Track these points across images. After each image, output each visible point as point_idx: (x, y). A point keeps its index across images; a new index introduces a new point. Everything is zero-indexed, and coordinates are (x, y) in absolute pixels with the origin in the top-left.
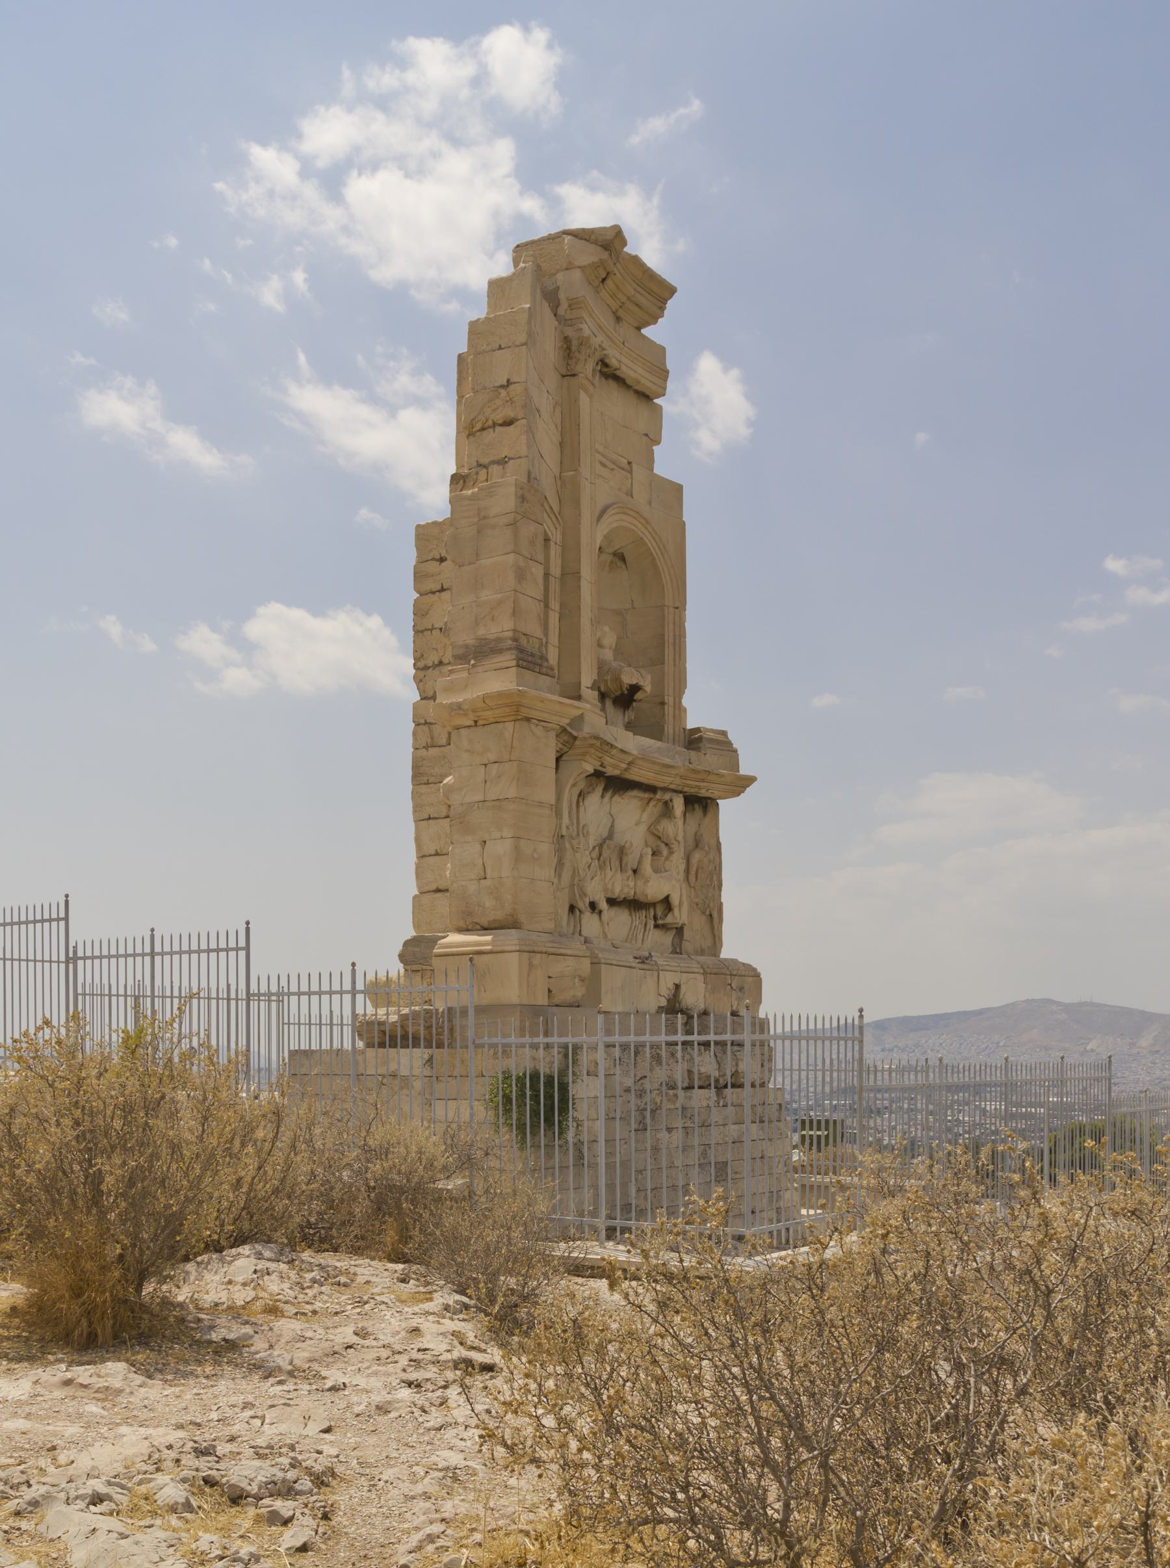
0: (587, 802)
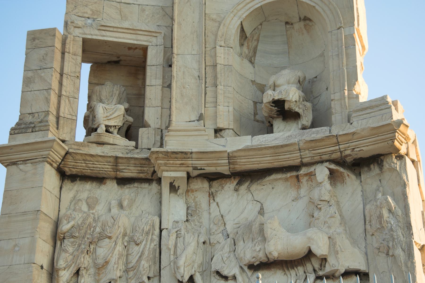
0: (217, 199)
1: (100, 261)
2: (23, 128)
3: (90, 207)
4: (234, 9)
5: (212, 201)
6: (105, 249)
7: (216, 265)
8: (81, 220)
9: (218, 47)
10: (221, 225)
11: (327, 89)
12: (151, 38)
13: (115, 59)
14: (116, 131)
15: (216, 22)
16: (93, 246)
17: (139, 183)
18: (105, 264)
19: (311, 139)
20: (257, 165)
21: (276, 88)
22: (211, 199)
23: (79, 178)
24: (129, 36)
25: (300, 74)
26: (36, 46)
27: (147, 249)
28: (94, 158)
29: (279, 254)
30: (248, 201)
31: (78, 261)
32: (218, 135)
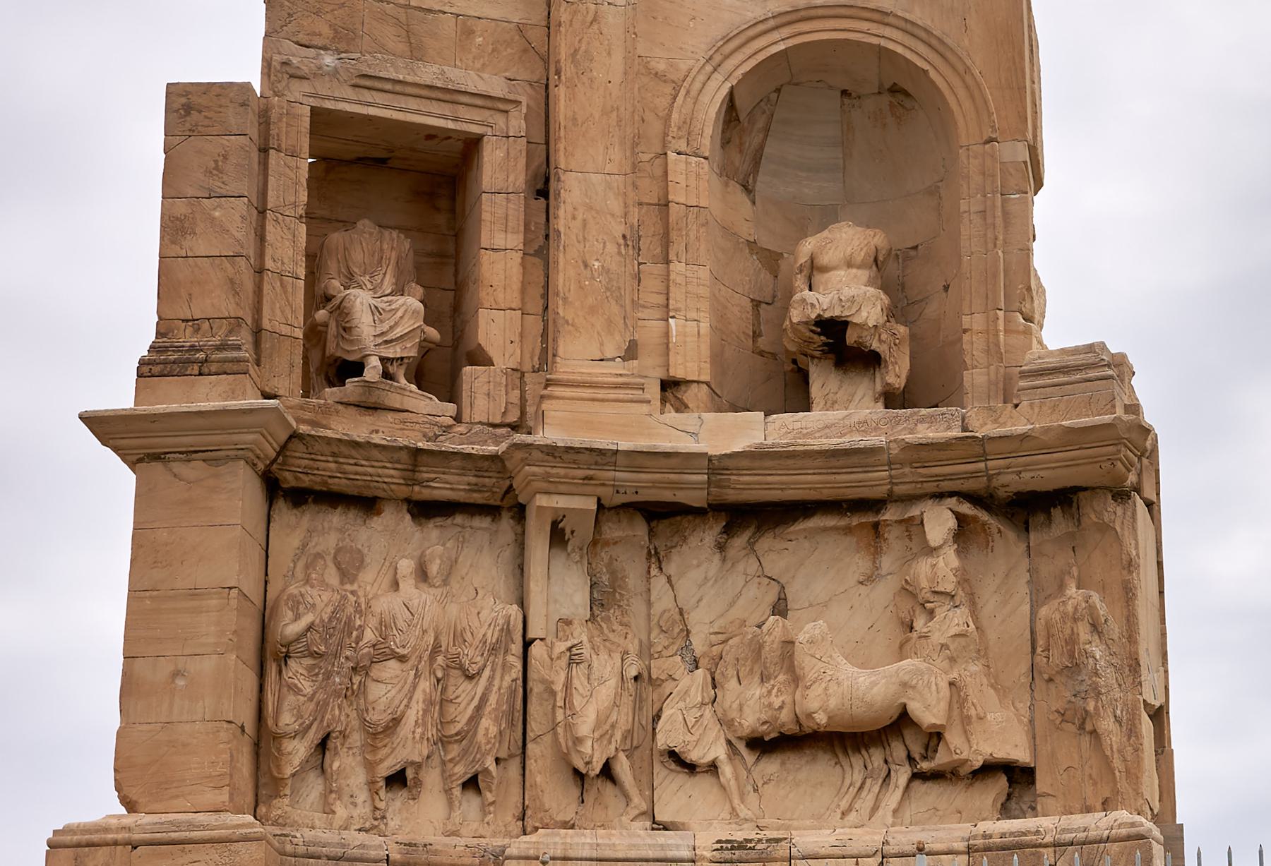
0: (671, 568)
1: (378, 717)
2: (174, 362)
3: (347, 575)
4: (716, 51)
5: (657, 570)
6: (390, 687)
7: (669, 735)
8: (330, 609)
9: (672, 156)
10: (679, 634)
11: (946, 288)
12: (491, 116)
13: (384, 155)
14: (401, 374)
15: (665, 81)
16: (359, 678)
17: (466, 516)
18: (391, 724)
19: (921, 441)
20: (779, 492)
21: (815, 273)
22: (653, 566)
23: (312, 496)
24: (435, 107)
25: (878, 239)
26: (194, 131)
27: (495, 689)
28: (361, 451)
29: (829, 718)
30: (749, 578)
31: (328, 716)
32: (669, 394)
